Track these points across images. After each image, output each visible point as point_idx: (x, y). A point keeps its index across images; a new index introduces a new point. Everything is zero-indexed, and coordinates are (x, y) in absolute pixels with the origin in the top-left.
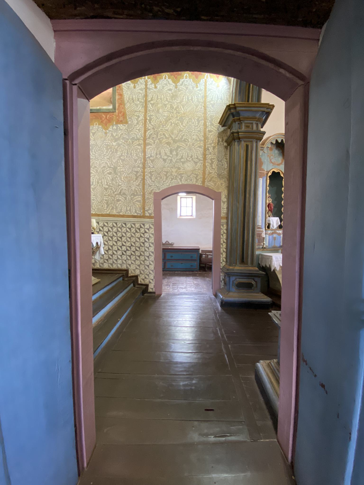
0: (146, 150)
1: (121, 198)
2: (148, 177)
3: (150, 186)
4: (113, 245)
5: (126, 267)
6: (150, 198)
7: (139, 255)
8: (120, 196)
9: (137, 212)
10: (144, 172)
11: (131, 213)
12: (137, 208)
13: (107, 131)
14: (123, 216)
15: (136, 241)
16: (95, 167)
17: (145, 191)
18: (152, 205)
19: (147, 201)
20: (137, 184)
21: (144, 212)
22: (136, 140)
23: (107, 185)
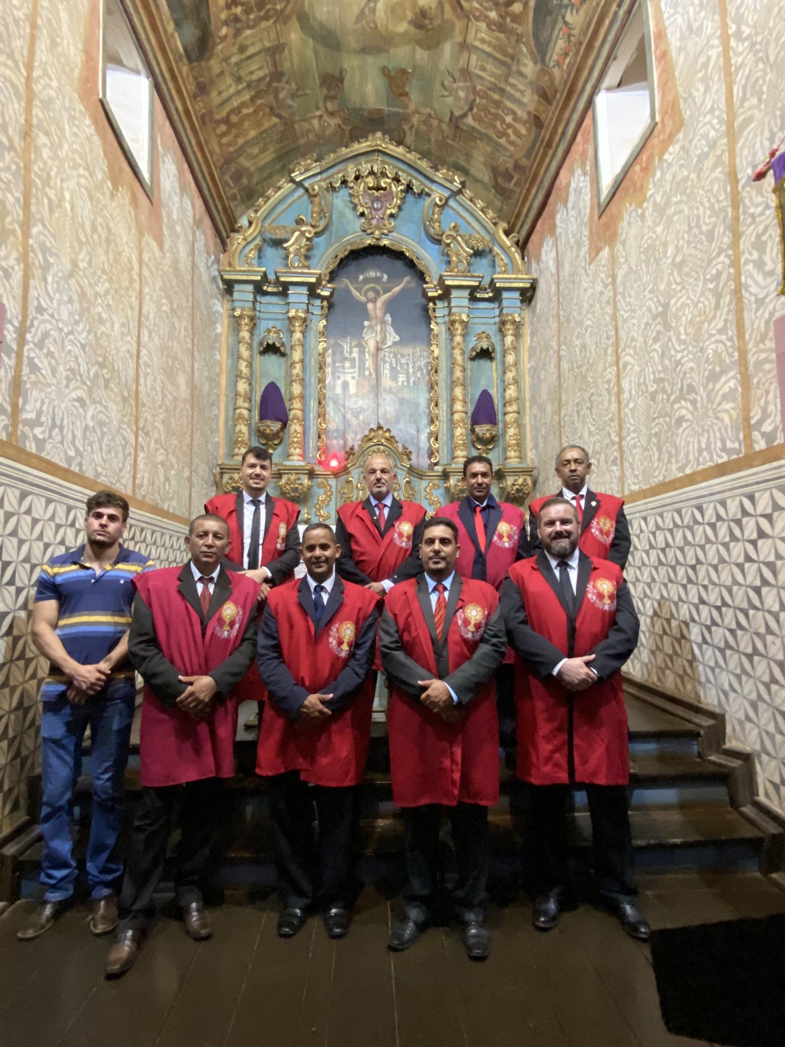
0: (738, 160)
1: (684, 409)
2: (750, 267)
3: (760, 302)
4: (680, 599)
5: (716, 702)
6: (766, 360)
7: (749, 650)
8: (683, 403)
9: (729, 445)
10: (735, 263)
11: (711, 459)
12: (726, 430)
13: (645, 204)
14: (691, 479)
15: (735, 582)
16: (633, 339)
17: (747, 337)
18: (774, 388)
19: (755, 381)
20: (721, 324)
21: (748, 438)
22: (707, 155)
23: (656, 381)
